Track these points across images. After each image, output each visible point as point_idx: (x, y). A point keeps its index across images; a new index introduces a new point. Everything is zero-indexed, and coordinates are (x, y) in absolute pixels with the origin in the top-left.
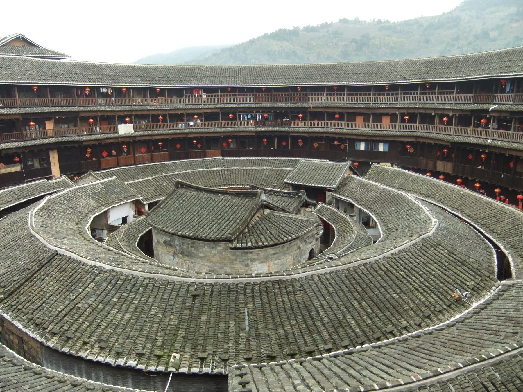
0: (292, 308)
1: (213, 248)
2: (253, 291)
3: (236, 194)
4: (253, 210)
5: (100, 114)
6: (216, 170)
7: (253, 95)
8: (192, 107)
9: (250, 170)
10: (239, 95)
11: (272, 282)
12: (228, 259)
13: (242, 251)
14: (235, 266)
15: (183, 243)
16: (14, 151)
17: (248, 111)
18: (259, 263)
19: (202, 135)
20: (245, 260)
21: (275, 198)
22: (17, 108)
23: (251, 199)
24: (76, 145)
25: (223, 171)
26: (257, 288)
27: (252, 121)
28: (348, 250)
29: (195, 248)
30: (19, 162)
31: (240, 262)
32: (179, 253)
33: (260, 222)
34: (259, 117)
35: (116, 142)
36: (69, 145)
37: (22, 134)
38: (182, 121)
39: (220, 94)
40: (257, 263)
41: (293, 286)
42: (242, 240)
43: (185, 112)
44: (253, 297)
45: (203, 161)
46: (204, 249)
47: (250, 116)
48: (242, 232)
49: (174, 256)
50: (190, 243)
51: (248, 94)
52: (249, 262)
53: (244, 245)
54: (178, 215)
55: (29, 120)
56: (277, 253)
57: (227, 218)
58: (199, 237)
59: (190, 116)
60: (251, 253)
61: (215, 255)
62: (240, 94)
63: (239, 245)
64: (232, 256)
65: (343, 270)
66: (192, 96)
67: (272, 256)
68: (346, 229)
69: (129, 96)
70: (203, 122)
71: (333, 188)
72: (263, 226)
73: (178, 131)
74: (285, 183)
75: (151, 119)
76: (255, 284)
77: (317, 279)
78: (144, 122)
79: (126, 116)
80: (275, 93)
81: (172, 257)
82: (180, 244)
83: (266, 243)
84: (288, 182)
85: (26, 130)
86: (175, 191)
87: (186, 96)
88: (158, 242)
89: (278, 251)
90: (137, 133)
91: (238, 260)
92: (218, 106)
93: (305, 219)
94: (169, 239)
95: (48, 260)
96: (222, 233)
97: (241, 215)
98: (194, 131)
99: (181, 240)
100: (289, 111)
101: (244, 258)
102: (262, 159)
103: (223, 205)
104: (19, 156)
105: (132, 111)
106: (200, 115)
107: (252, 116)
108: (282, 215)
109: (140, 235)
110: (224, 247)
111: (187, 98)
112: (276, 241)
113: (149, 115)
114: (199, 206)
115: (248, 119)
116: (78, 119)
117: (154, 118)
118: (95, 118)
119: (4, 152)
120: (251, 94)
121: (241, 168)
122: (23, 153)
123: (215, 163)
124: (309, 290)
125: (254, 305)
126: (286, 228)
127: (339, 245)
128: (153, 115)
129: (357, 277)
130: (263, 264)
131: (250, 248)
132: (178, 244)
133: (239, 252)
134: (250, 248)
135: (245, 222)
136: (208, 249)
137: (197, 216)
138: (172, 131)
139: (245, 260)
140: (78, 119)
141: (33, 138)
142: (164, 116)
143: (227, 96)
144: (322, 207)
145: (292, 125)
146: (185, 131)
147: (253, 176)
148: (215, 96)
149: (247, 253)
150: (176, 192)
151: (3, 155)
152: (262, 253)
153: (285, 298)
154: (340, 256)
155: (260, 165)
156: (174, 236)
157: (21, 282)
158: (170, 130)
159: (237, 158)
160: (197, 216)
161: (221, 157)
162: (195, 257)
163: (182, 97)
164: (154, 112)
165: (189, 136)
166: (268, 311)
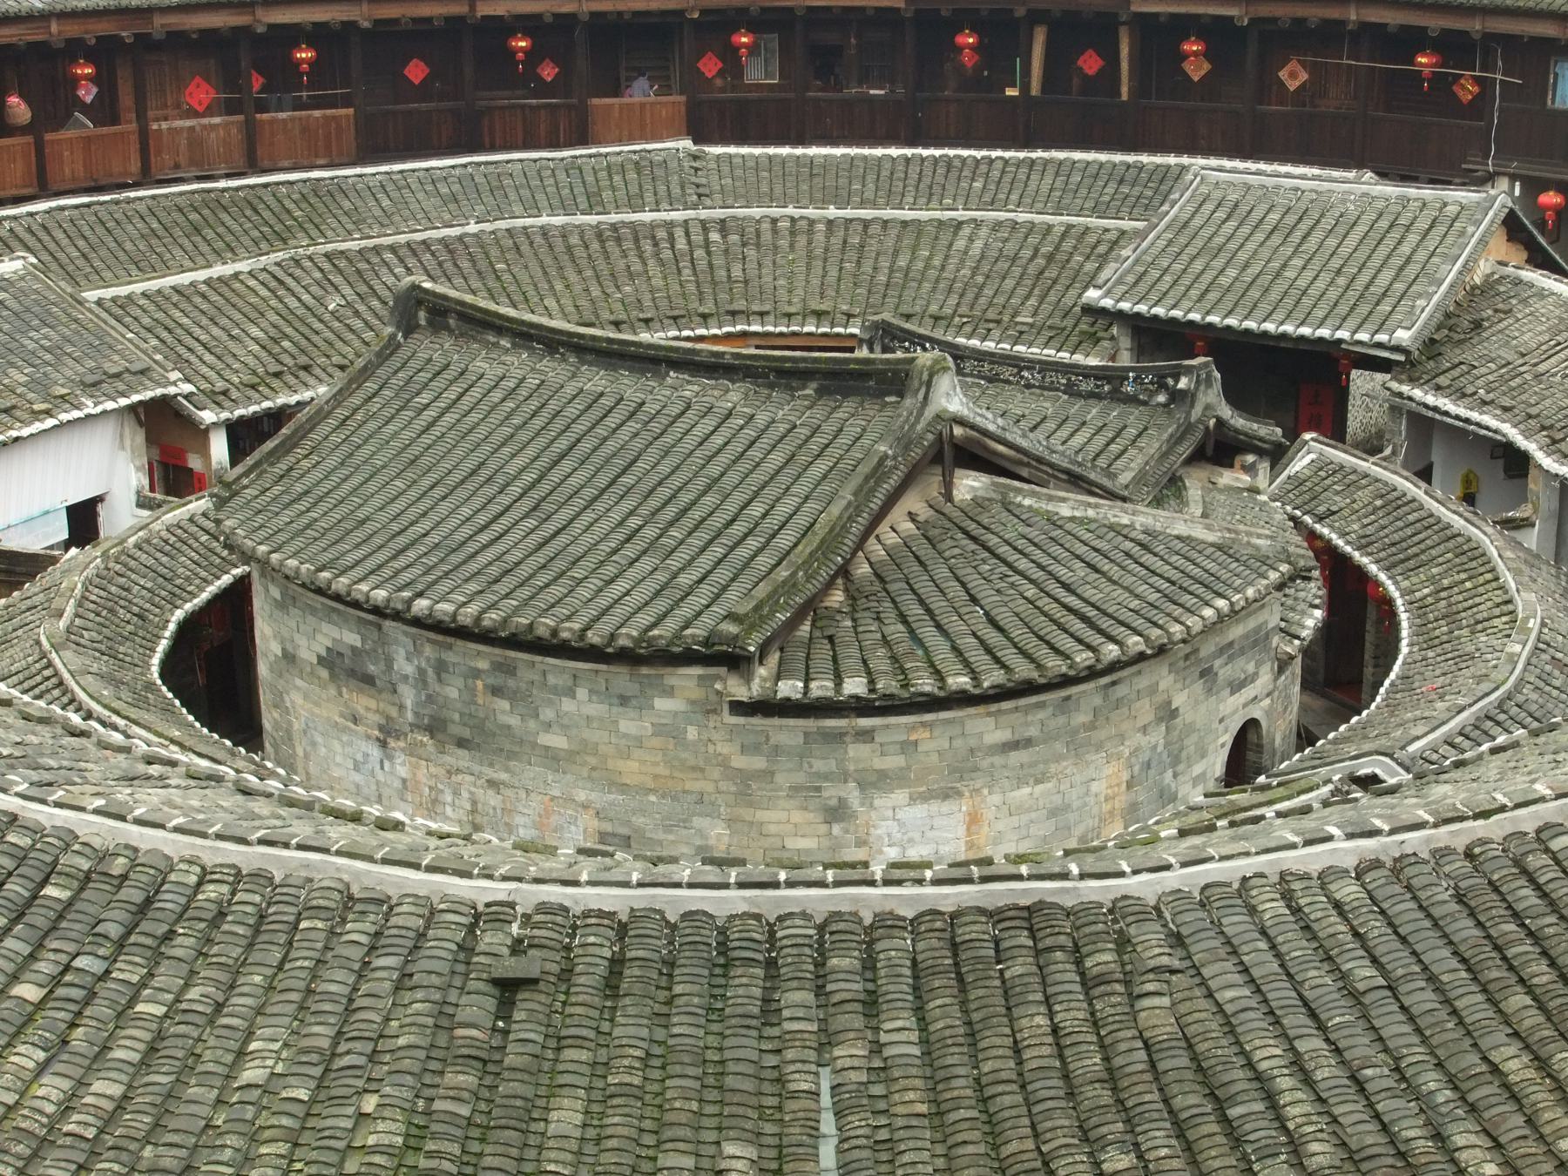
0: (1112, 1077)
1: (624, 700)
2: (869, 964)
3: (776, 373)
4: (878, 473)
6: (653, 226)
9: (866, 224)
11: (996, 916)
12: (716, 773)
13: (810, 724)
14: (762, 815)
15: (441, 668)
18: (913, 799)
20: (826, 777)
21: (1020, 403)
23: (871, 408)
25: (695, 230)
26: (893, 950)
28: (1476, 732)
29: (514, 697)
31: (795, 789)
32: (415, 727)
33: (925, 551)
40: (900, 796)
41: (1123, 943)
42: (806, 654)
44: (871, 1004)
45: (572, 166)
46: (567, 705)
48: (810, 607)
49: (383, 744)
50: (483, 665)
52: (852, 793)
53: (821, 688)
54: (413, 494)
56: (1028, 743)
57: (717, 521)
58: (542, 631)
60: (866, 736)
61: (639, 742)
63: (790, 688)
64: (744, 749)
65: (1441, 854)
67: (998, 760)
68: (1469, 602)
71: (1397, 349)
72: (942, 572)
74: (1091, 311)
76: (887, 923)
77: (1272, 908)
81: (375, 752)
82: (422, 672)
83: (959, 681)
84: (1107, 303)
86: (391, 347)
88: (289, 658)
89: (1033, 732)
91: (781, 779)
93: (1211, 537)
94: (352, 638)
96: (685, 611)
97: (812, 503)
99: (428, 650)
101: (819, 765)
102: (949, 162)
103: (690, 442)
108: (1068, 505)
109: (179, 614)
110: (697, 693)
112: (1024, 670)
114: (542, 441)
121: (811, 212)
123: (648, 181)
124: (1222, 974)
125: (877, 1048)
126: (1089, 592)
127: (1417, 706)
129: (1527, 897)
130: (935, 806)
131: (861, 707)
132: (409, 669)
133: (788, 731)
134: (861, 707)
135: (827, 546)
136: (596, 709)
137: (526, 504)
139: (826, 777)
144: (1320, 465)
147: (884, 263)
149: (838, 737)
150: (404, 353)
152: (933, 736)
153: (1072, 1016)
154: (1424, 772)
155: (930, 197)
156: (388, 624)
159: (785, 151)
160: (526, 504)
161: (687, 144)
162: (512, 756)
166: (961, 1088)
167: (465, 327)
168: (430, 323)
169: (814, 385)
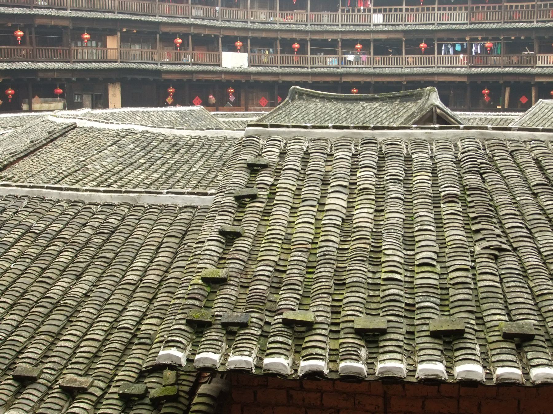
5: (192, 31)
7: (466, 9)
8: (352, 28)
10: (439, 9)
16: (56, 75)
17: (455, 37)
19: (368, 79)
22: (66, 10)
24: (151, 78)
27: (461, 56)
30: (62, 96)
34: (477, 48)
35: (217, 81)
36: (140, 77)
37: (70, 51)
38: (335, 53)
39: (404, 7)
43: (339, 37)
47: (458, 48)
51: (458, 6)
55: (82, 30)
59: (349, 45)
62: (442, 6)
66: (353, 11)
69: (245, 7)
70: (372, 56)
73: (326, 70)
75: (279, 49)
78: (267, 52)
79: (236, 39)
80: (509, 4)
85: (77, 46)
87: (343, 11)
90: (253, 69)
92: (400, 28)
95: (61, 133)
98: (355, 70)
100: (533, 37)
103: (362, 115)
104: (62, 87)
105: (248, 30)
106: (366, 44)
107: (462, 46)
111: (345, 13)
113: (276, 39)
115: (455, 52)
116: (158, 36)
117: (285, 44)
118: (184, 36)
119: (41, 75)
120: (463, 6)
122: (69, 80)
128: (283, 40)
138: (315, 70)
140: (158, 36)
141: (86, 57)
142: (303, 43)
143: (417, 10)
145: (539, 64)
146: (339, 70)
148: (396, 10)
150: (290, 105)
151: (39, 79)
157: (18, 156)
158: (312, 68)
163: (337, 11)
164: (285, 36)
165: (345, 79)
167: (307, 98)
168: (299, 98)
169: (398, 100)
